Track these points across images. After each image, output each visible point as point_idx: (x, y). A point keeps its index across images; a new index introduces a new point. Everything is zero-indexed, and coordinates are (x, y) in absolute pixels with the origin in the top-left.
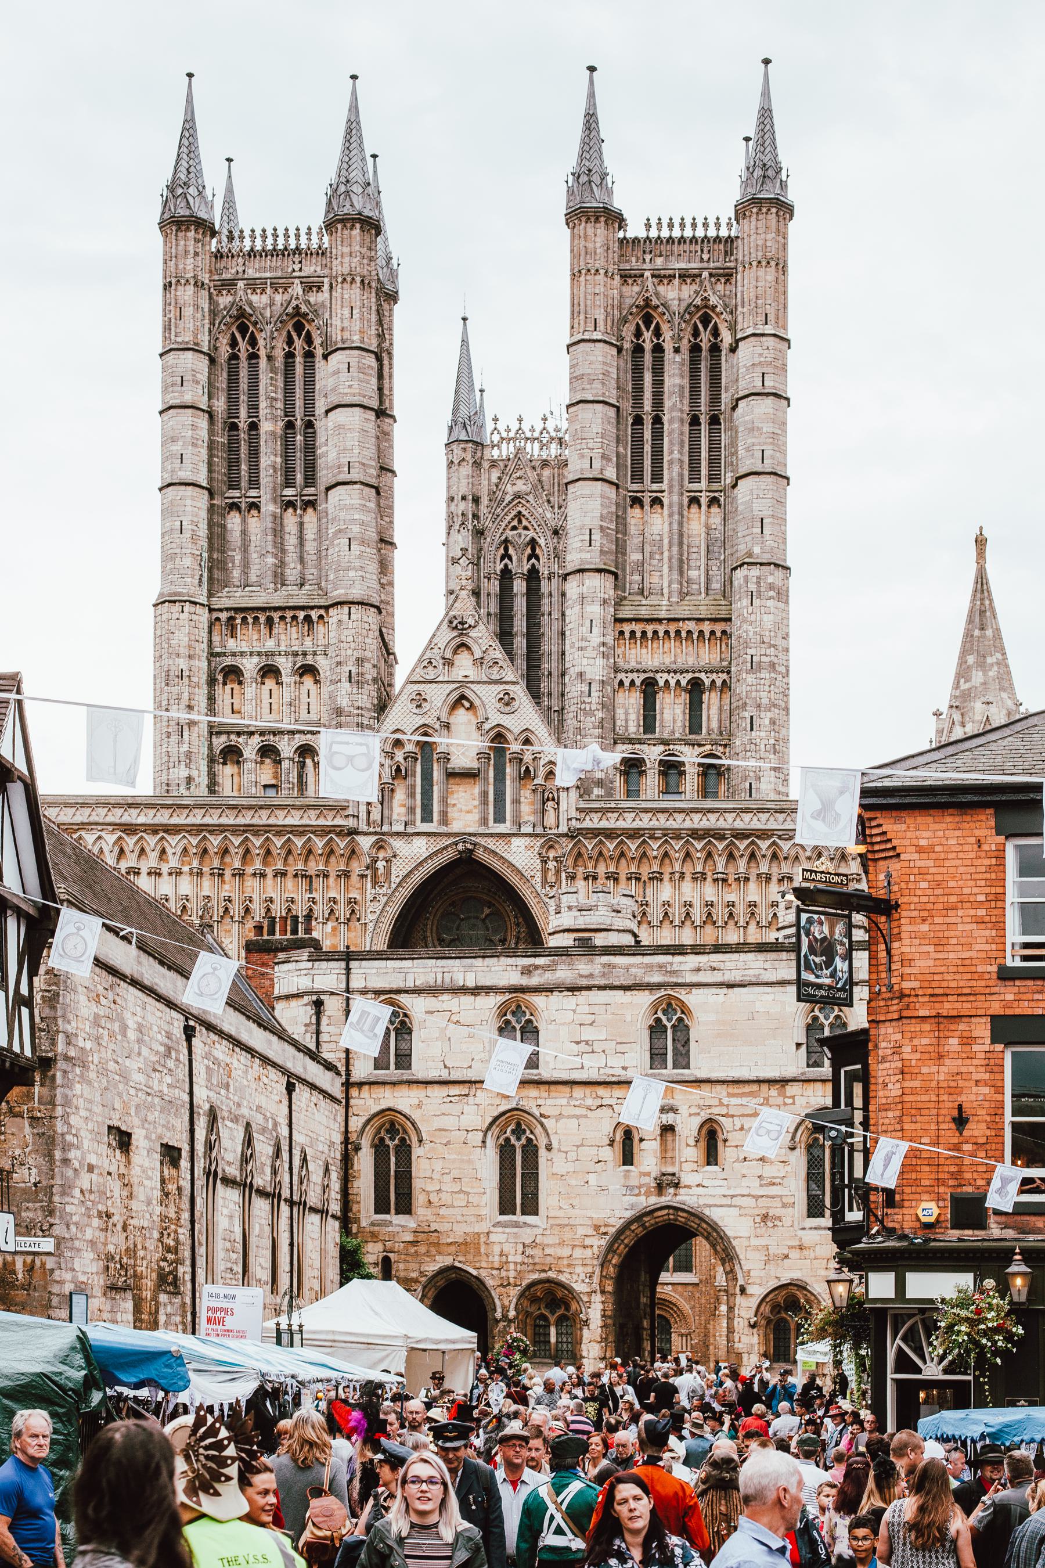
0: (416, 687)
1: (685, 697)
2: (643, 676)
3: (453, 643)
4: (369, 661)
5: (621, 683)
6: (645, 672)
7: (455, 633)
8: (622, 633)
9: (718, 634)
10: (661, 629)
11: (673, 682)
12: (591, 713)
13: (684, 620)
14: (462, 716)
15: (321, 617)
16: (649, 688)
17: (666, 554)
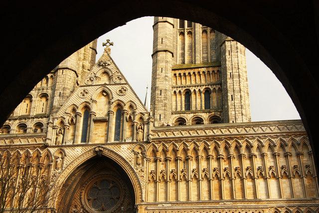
0: (83, 88)
1: (203, 95)
2: (184, 89)
3: (101, 71)
4: (69, 89)
5: (175, 92)
6: (185, 87)
7: (101, 67)
8: (175, 74)
9: (216, 72)
10: (192, 72)
11: (197, 90)
12: (161, 101)
13: (201, 68)
14: (103, 100)
15: (52, 76)
16: (188, 94)
17: (193, 48)
